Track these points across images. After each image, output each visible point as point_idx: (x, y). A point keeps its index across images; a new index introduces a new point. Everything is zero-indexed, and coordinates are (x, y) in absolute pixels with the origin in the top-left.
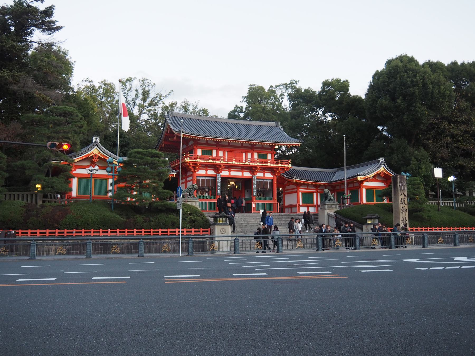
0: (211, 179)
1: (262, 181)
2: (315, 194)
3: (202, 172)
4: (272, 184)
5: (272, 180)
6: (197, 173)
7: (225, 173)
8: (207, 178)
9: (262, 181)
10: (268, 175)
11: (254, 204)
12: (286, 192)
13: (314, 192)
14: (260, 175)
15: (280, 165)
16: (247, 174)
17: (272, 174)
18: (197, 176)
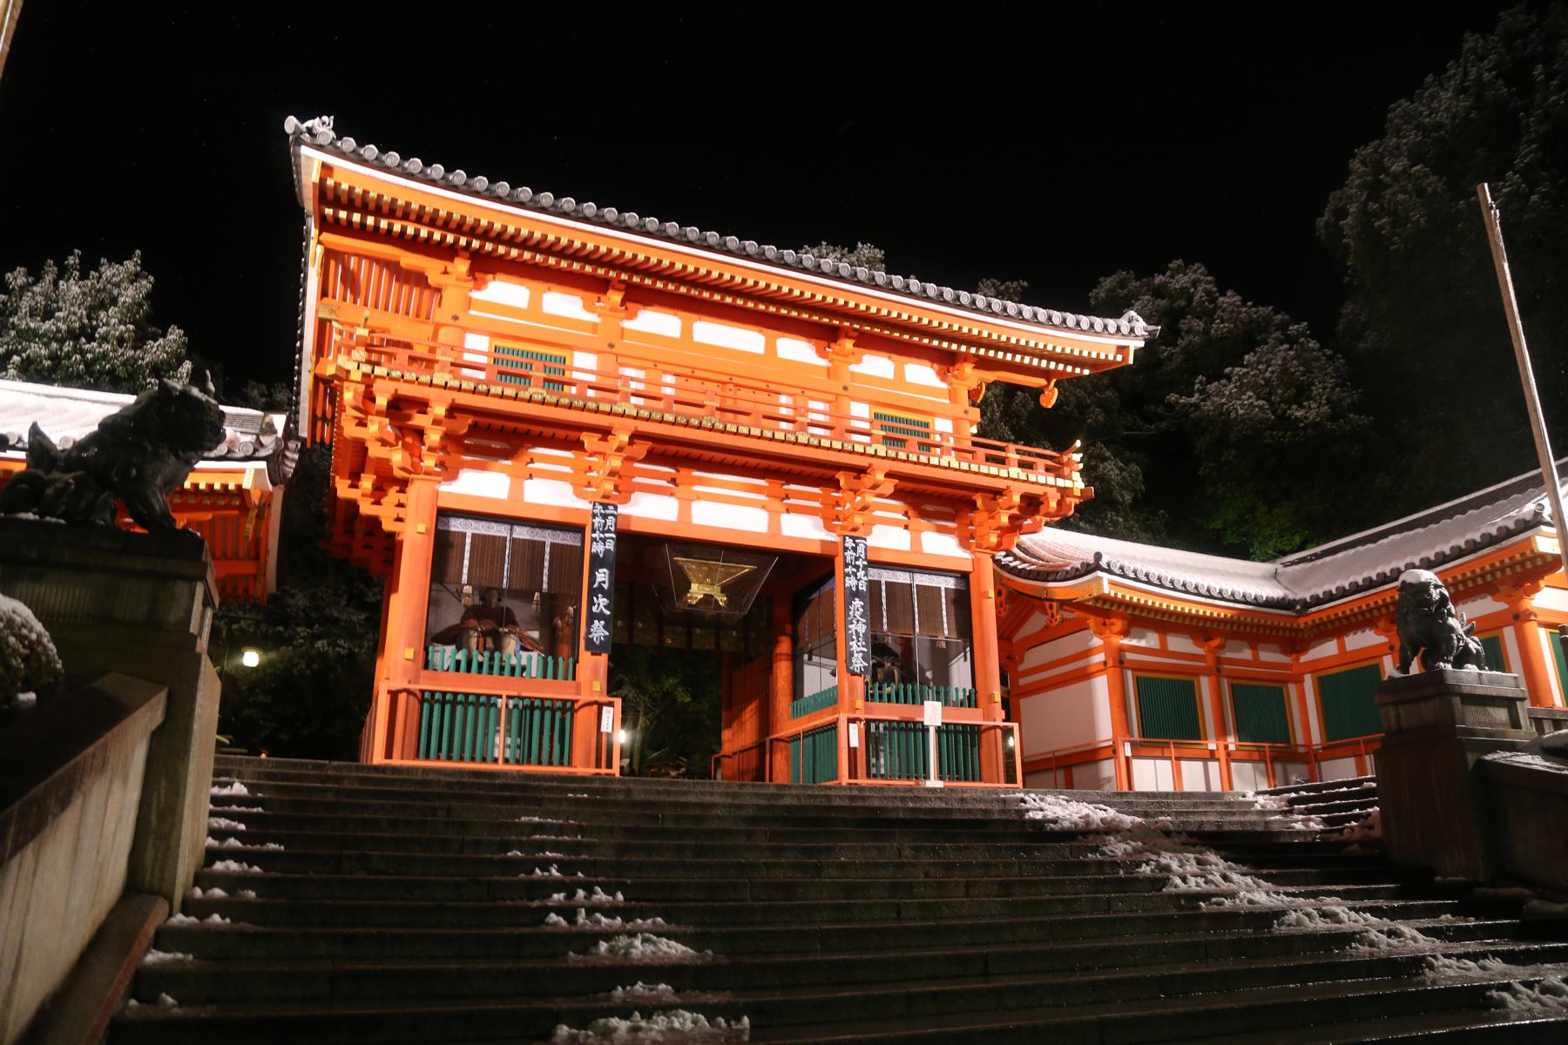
0: (548, 538)
1: (902, 578)
2: (1205, 684)
3: (482, 484)
4: (962, 600)
5: (964, 577)
6: (445, 488)
7: (652, 509)
8: (522, 533)
9: (902, 578)
10: (941, 545)
11: (854, 729)
12: (1023, 681)
13: (1197, 673)
14: (891, 535)
15: (1015, 472)
16: (802, 530)
17: (964, 544)
18: (444, 513)
